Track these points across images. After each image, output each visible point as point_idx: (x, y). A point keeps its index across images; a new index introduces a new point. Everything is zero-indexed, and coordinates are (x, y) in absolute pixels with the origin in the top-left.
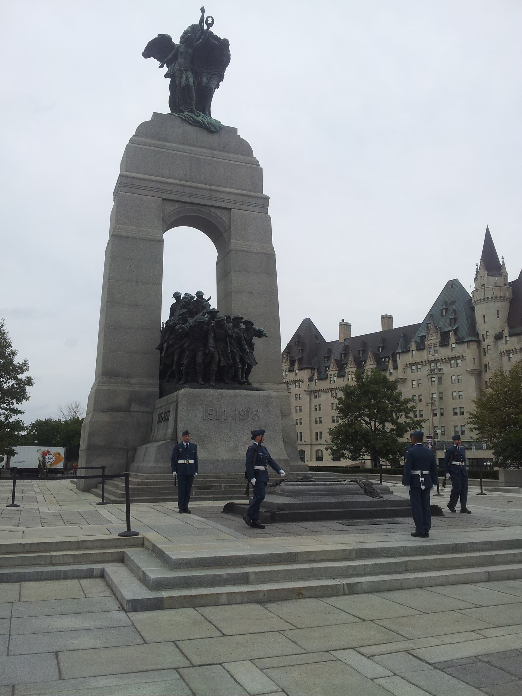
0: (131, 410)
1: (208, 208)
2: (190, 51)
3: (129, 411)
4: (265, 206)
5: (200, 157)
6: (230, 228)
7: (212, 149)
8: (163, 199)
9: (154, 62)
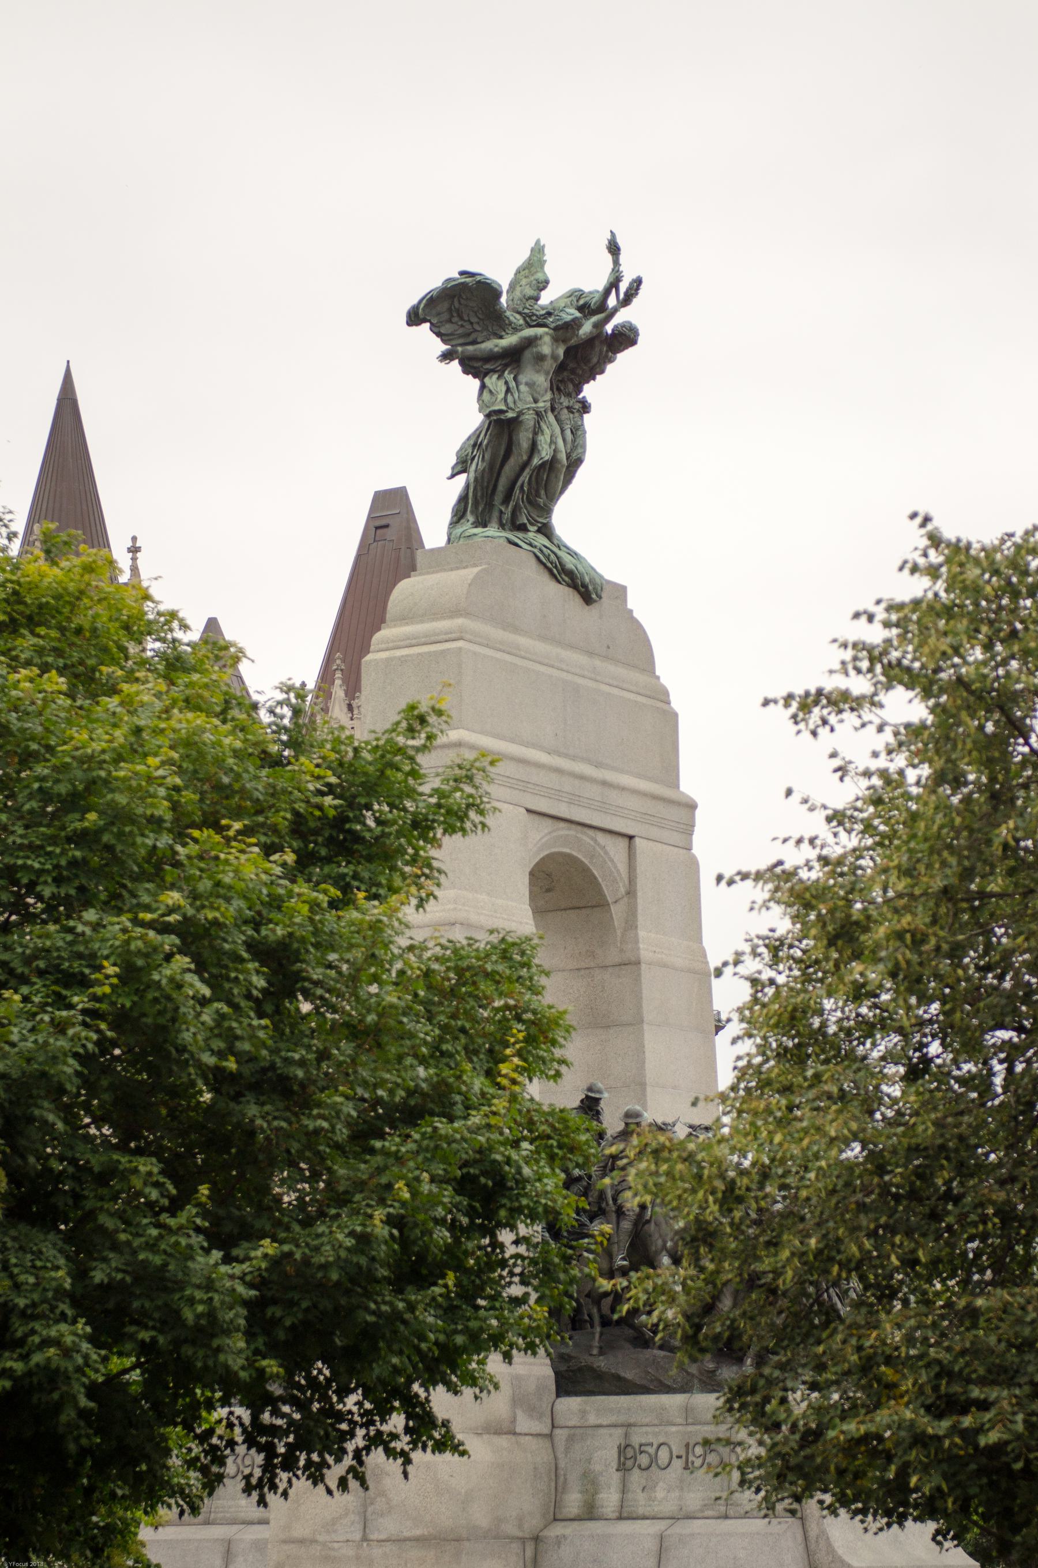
0: (518, 1430)
1: (591, 832)
2: (561, 352)
3: (515, 1434)
4: (688, 829)
5: (580, 681)
6: (631, 892)
7: (591, 654)
8: (528, 811)
9: (427, 342)
